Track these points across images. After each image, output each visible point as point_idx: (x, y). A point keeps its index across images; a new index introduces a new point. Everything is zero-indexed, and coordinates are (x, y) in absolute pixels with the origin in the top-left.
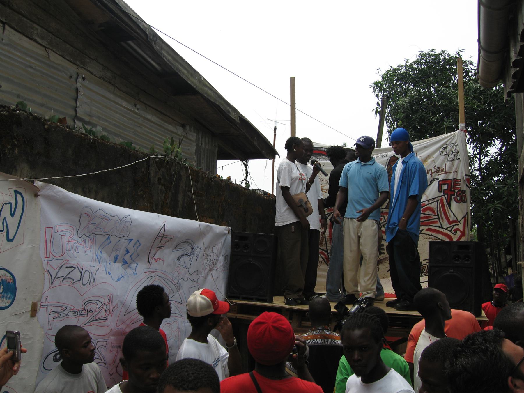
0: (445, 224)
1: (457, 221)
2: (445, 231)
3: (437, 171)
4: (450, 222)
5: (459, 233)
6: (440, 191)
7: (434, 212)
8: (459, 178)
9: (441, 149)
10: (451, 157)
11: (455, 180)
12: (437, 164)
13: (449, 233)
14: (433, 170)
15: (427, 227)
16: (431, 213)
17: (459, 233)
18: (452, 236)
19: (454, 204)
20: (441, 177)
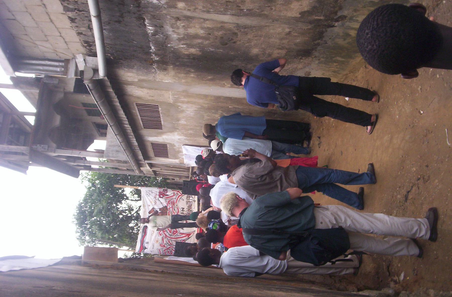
0: (175, 197)
1: (174, 193)
2: (177, 197)
3: (155, 198)
4: (174, 195)
5: (178, 193)
6: (163, 198)
7: (170, 201)
8: (158, 191)
9: (147, 196)
10: (151, 193)
11: (159, 192)
12: (153, 198)
13: (178, 196)
14: (155, 199)
15: (175, 203)
16: (170, 202)
17: (178, 193)
18: (179, 195)
19: (167, 194)
20: (158, 197)
